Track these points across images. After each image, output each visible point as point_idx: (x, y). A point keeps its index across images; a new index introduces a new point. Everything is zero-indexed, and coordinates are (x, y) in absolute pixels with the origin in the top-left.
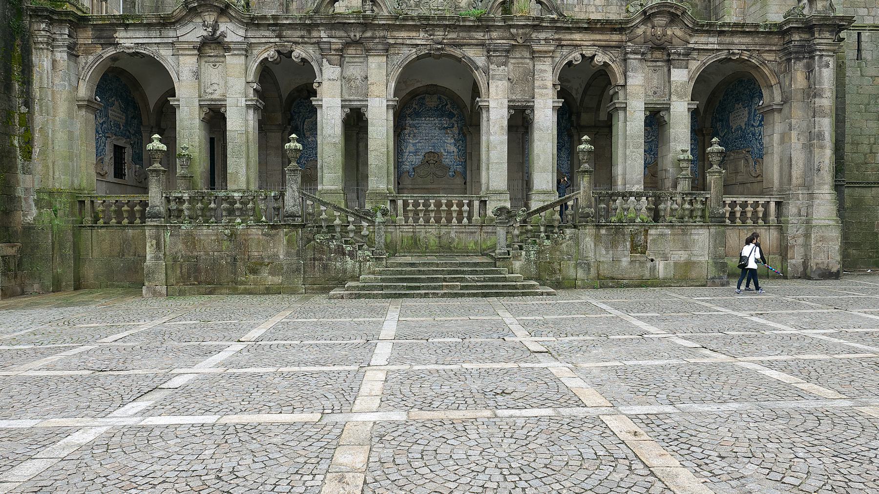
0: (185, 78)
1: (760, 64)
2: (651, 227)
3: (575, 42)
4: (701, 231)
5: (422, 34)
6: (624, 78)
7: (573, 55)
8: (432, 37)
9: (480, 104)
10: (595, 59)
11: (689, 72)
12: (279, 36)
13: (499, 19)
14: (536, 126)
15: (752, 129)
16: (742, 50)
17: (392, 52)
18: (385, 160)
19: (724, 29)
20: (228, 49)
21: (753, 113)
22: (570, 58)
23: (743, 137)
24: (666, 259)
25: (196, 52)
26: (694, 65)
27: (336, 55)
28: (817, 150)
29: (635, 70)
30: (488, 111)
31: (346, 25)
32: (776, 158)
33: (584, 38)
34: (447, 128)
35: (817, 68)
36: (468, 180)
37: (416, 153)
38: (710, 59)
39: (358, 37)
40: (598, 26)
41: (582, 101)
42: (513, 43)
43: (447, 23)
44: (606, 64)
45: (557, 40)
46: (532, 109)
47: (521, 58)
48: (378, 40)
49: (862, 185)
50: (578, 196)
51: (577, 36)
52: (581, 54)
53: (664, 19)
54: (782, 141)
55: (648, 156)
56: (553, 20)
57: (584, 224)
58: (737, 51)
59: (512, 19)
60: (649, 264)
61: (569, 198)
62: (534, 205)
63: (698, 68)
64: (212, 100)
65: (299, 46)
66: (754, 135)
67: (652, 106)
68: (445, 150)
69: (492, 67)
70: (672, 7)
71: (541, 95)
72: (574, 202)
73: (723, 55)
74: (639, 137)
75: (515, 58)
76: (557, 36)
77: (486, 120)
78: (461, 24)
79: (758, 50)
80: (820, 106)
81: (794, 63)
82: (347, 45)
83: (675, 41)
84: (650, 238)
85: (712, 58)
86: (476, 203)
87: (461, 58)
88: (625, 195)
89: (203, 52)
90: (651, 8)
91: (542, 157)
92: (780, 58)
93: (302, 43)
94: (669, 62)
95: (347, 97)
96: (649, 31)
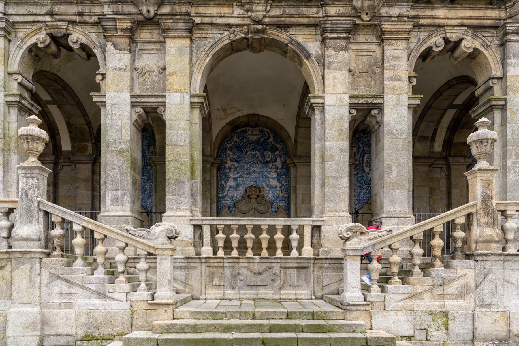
3: (437, 21)
5: (238, 11)
9: (312, 101)
10: (463, 43)
12: (51, 14)
14: (386, 128)
17: (198, 36)
45: (414, 17)
65: (77, 27)
69: (330, 52)
71: (393, 89)
76: (413, 13)
77: (320, 123)
86: (307, 231)
87: (287, 45)
93: (80, 22)
95: (138, 92)
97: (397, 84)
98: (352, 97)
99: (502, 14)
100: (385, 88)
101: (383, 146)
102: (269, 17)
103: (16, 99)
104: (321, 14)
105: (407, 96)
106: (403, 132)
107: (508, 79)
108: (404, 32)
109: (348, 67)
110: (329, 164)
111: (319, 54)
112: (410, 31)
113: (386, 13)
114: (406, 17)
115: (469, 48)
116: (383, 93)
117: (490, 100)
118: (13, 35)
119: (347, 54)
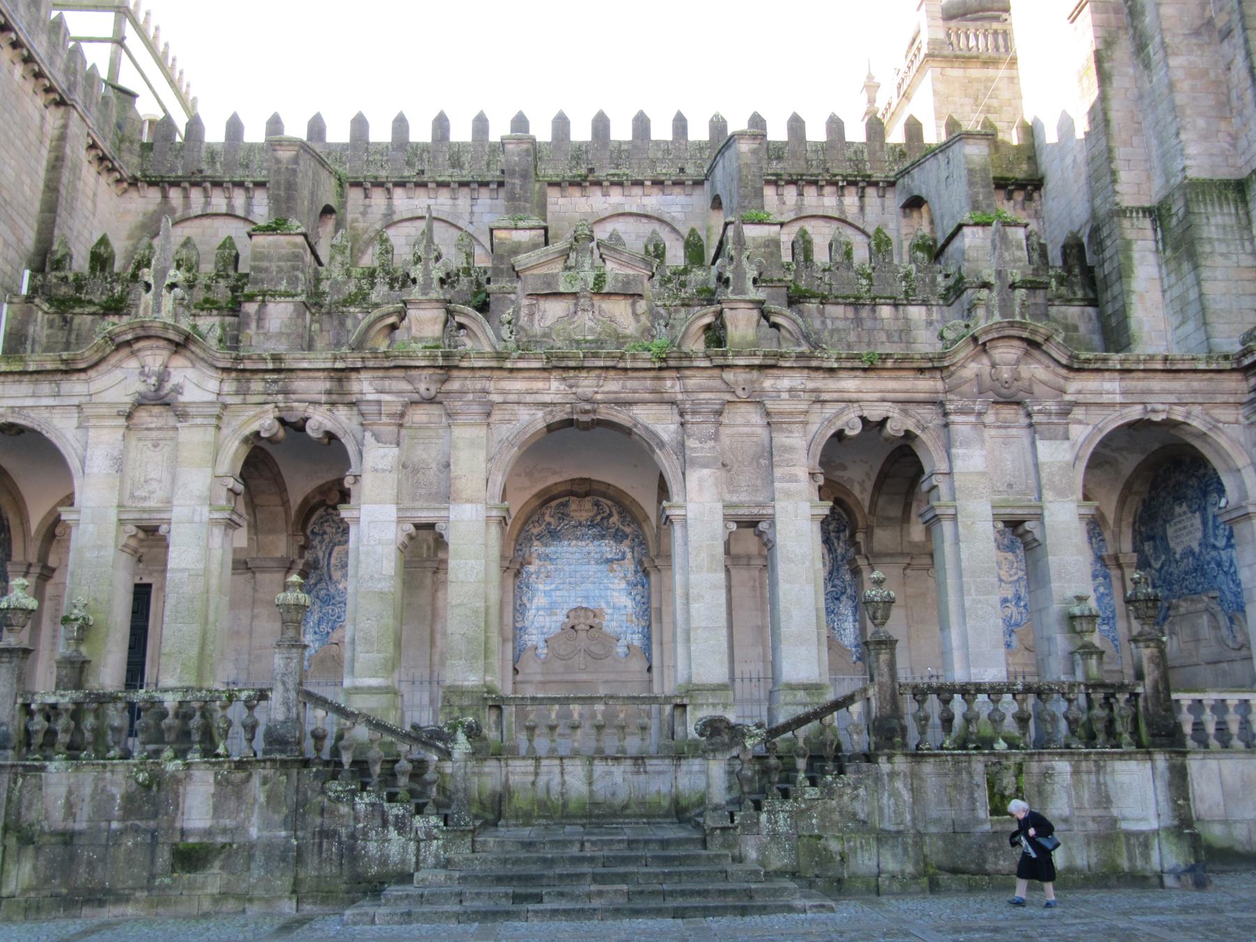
0: (95, 470)
3: (846, 396)
4: (1132, 765)
5: (555, 385)
7: (845, 419)
8: (574, 390)
9: (668, 512)
10: (888, 425)
11: (1073, 446)
15: (1214, 553)
17: (499, 417)
18: (483, 624)
19: (1127, 366)
20: (182, 415)
21: (1210, 523)
22: (839, 424)
23: (1199, 569)
25: (122, 421)
27: (389, 424)
29: (966, 444)
30: (685, 525)
31: (414, 373)
33: (863, 388)
34: (609, 561)
36: (655, 663)
37: (551, 610)
38: (1114, 420)
39: (433, 392)
41: (873, 504)
42: (728, 397)
43: (601, 364)
44: (909, 435)
45: (813, 391)
46: (772, 520)
47: (745, 425)
48: (470, 396)
51: (850, 384)
55: (1014, 609)
56: (800, 356)
58: (1160, 407)
63: (1088, 439)
64: (144, 511)
66: (1219, 565)
67: (1008, 511)
68: (607, 603)
71: (788, 494)
73: (1135, 413)
78: (629, 365)
79: (1200, 404)
82: (413, 403)
83: (1037, 389)
89: (135, 420)
92: (1247, 418)
94: (1031, 425)
95: (407, 503)
97: (793, 486)
102: (603, 393)
103: (226, 515)
104: (677, 388)
107: (956, 477)
108: (801, 413)
110: (695, 607)
115: (898, 431)
116: (773, 500)
118: (225, 419)
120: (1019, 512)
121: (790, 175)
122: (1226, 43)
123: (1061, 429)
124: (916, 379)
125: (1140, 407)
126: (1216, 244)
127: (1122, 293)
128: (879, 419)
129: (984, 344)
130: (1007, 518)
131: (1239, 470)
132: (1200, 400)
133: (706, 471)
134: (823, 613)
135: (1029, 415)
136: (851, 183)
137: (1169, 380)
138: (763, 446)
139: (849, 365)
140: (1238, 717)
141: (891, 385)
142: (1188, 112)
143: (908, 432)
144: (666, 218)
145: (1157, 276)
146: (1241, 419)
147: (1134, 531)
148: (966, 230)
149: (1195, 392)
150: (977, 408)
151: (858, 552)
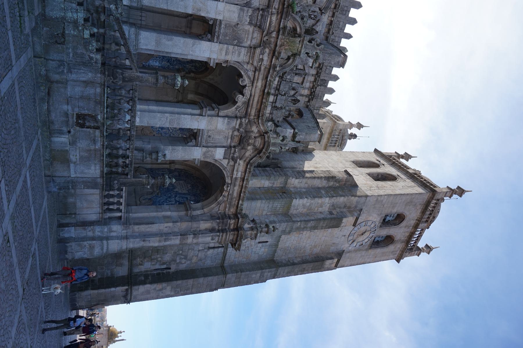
1: (218, 202)
2: (102, 132)
3: (255, 81)
6: (223, 115)
7: (246, 79)
11: (220, 160)
13: (286, 24)
14: (197, 41)
16: (229, 191)
22: (245, 77)
24: (73, 143)
26: (225, 162)
28: (158, 239)
29: (228, 123)
32: (154, 214)
35: (212, 234)
40: (264, 101)
42: (265, 33)
44: (235, 103)
45: (260, 68)
46: (211, 40)
47: (252, 37)
49: (130, 257)
50: (135, 71)
51: (259, 84)
52: (246, 86)
53: (259, 145)
54: (165, 217)
56: (275, 67)
57: (107, 73)
58: (229, 188)
59: (283, 34)
60: (65, 129)
61: (132, 61)
62: (125, 28)
63: (222, 165)
67: (201, 135)
69: (250, 11)
70: (266, 151)
71: (221, 50)
72: (128, 66)
73: (228, 180)
74: (178, 124)
75: (253, 32)
76: (263, 68)
79: (227, 200)
80: (187, 238)
81: (217, 222)
84: (91, 131)
85: (227, 174)
88: (132, 111)
90: (269, 137)
91: (170, 43)
94: (231, 147)
96: (253, 135)
97: (224, 53)
98: (220, 22)
99: (252, 117)
100: (223, 45)
101: (186, 38)
105: (216, 58)
106: (194, 52)
107: (217, 118)
108: (253, 62)
109: (239, 23)
111: (251, 5)
112: (252, 65)
113: (265, 52)
114: (261, 63)
116: (220, 43)
117: (206, 107)
119: (247, 23)
120: (200, 139)
121: (320, 73)
122: (328, 213)
123: (228, 157)
124: (256, 110)
125: (230, 182)
126: (272, 205)
127: (262, 176)
128: (244, 92)
129: (264, 135)
130: (198, 134)
131: (203, 209)
132: (228, 201)
133: (236, 15)
134: (168, 55)
135: (234, 147)
136: (311, 93)
137: (237, 193)
138: (242, 43)
139: (267, 85)
140: (116, 202)
141: (256, 99)
142: (312, 201)
143: (237, 102)
144: (318, 24)
145: (265, 186)
146: (220, 211)
147: (182, 169)
148: (292, 131)
149: (232, 199)
150: (241, 129)
151: (187, 73)
